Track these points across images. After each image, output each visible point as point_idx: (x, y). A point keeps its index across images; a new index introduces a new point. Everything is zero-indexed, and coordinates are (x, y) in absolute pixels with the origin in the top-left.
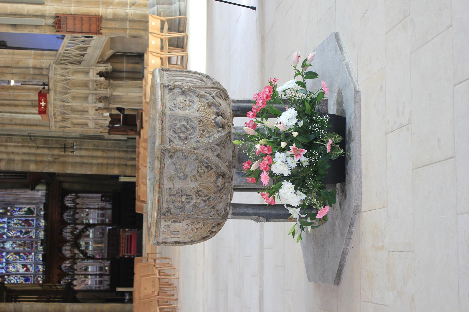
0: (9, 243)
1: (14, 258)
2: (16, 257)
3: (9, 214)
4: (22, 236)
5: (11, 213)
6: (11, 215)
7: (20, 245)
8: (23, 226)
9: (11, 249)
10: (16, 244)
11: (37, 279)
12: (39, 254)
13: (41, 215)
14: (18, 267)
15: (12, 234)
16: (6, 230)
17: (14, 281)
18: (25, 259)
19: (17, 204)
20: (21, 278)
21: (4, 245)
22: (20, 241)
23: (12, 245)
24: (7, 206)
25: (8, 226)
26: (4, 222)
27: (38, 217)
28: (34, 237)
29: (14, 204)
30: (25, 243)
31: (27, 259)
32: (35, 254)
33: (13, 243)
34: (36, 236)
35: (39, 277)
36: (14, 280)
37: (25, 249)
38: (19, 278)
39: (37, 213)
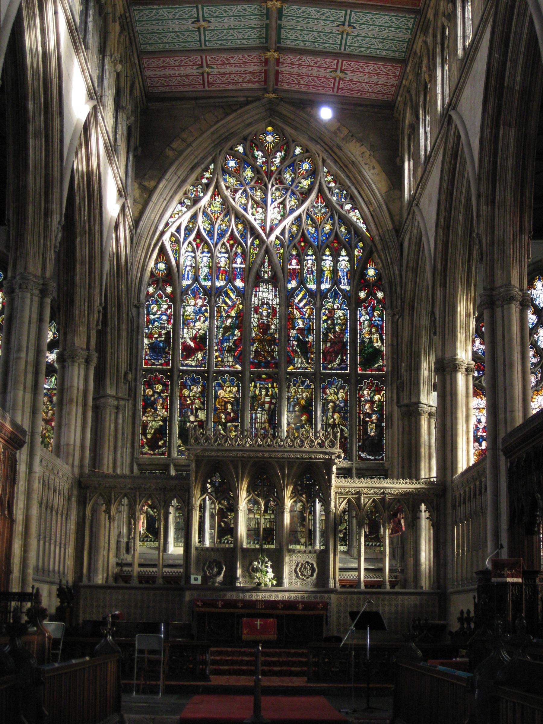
0: (271, 296)
1: (227, 312)
2: (228, 317)
3: (362, 295)
4: (293, 333)
5: (364, 300)
6: (359, 302)
7: (264, 328)
8: (326, 335)
9: (255, 301)
10: (267, 316)
11: (159, 381)
12: (238, 386)
13: (361, 389)
14: (198, 325)
15: (301, 305)
16: (312, 286)
17: (154, 315)
18: (221, 342)
19: (394, 315)
20: (163, 332)
21: (267, 282)
22: (279, 329)
23: (268, 304)
24: (387, 289)
25: (324, 295)
26: (336, 281)
27: (353, 380)
28: (291, 369)
29: (392, 307)
30: (272, 341)
31: (221, 350)
32: (235, 373)
33: (274, 309)
34: (291, 374)
35: (165, 385)
36: (159, 313)
37: (254, 340)
38: (163, 328)
39: (367, 377)
